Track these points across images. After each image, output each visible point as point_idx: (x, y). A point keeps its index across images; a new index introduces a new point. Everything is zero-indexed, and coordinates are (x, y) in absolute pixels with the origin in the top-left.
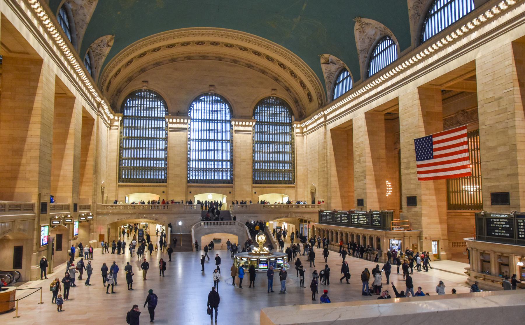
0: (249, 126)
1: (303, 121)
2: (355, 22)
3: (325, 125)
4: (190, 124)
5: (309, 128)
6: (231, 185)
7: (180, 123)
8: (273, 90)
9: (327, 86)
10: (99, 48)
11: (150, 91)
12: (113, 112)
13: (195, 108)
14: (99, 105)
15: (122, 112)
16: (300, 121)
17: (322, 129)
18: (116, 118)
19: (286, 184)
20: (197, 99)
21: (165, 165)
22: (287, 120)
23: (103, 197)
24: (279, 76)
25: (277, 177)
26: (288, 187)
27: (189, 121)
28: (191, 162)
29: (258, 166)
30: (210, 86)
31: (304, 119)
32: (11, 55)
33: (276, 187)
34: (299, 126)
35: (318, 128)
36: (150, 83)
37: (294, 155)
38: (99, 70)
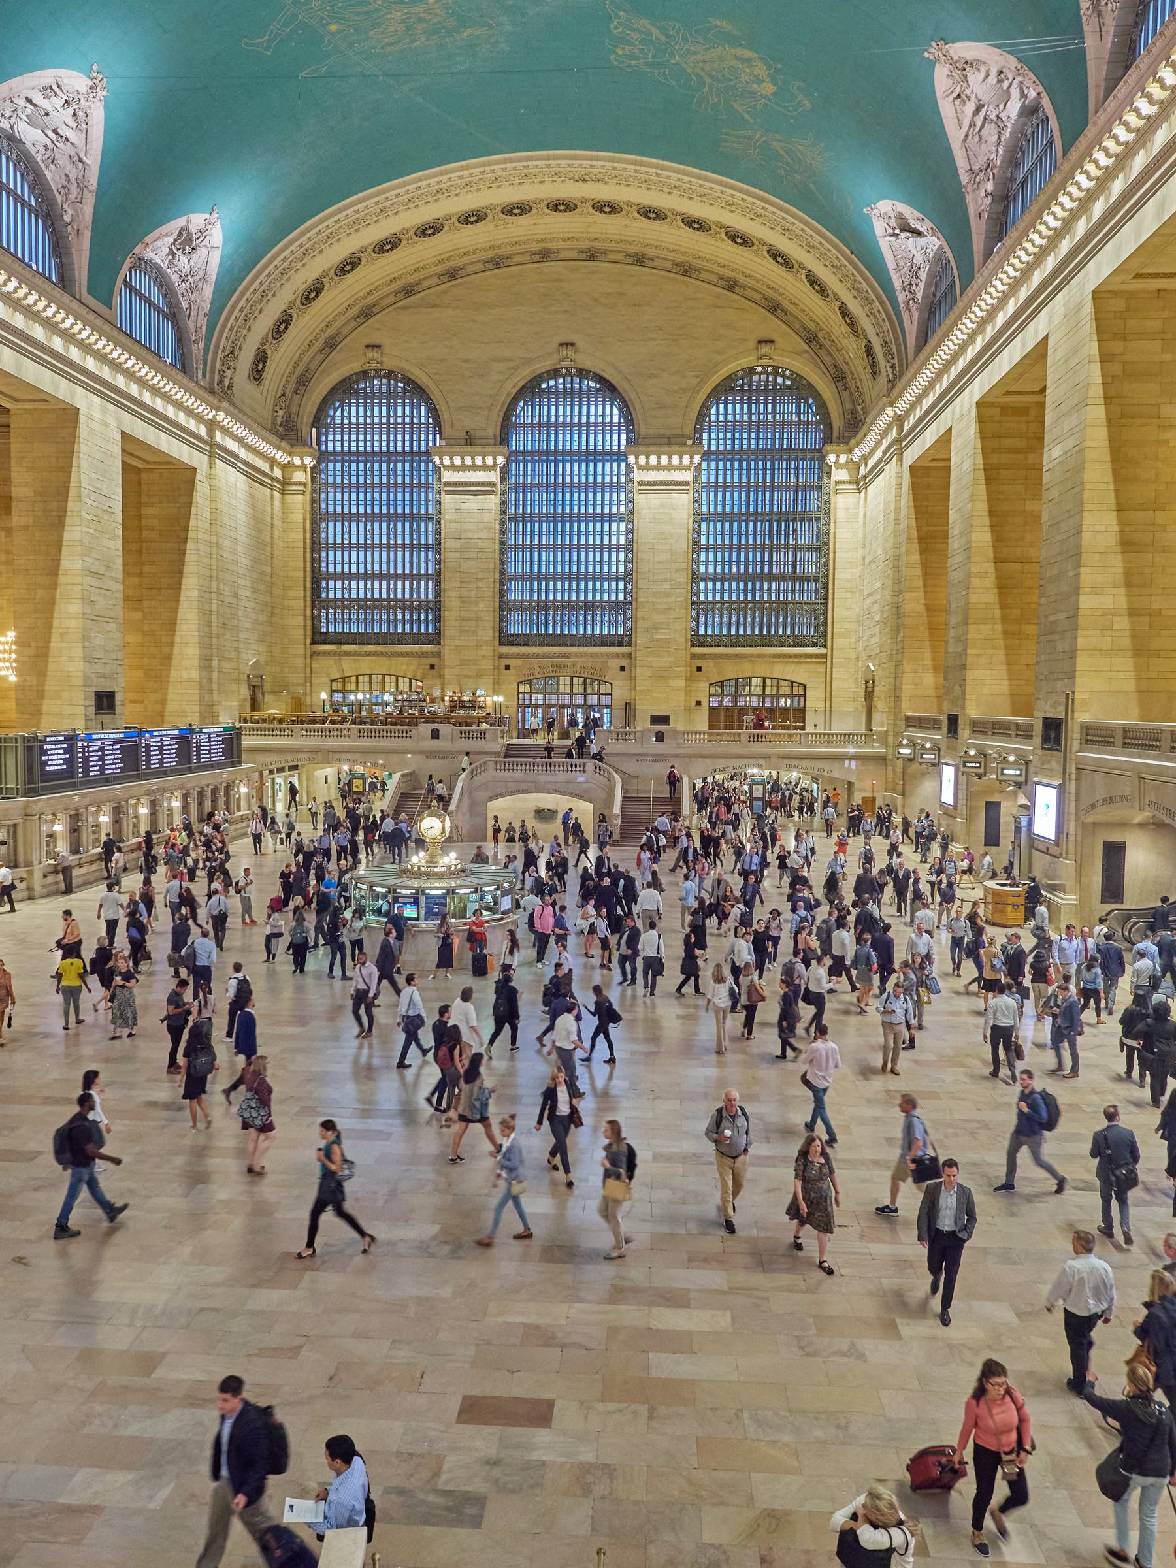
0: (680, 467)
1: (853, 441)
2: (932, 64)
5: (871, 463)
6: (625, 650)
7: (474, 468)
8: (760, 342)
9: (906, 316)
10: (183, 259)
11: (390, 375)
12: (284, 444)
14: (212, 425)
16: (847, 443)
17: (891, 468)
18: (297, 461)
20: (530, 390)
21: (438, 593)
22: (812, 440)
24: (781, 294)
29: (708, 592)
30: (561, 344)
34: (843, 459)
36: (387, 349)
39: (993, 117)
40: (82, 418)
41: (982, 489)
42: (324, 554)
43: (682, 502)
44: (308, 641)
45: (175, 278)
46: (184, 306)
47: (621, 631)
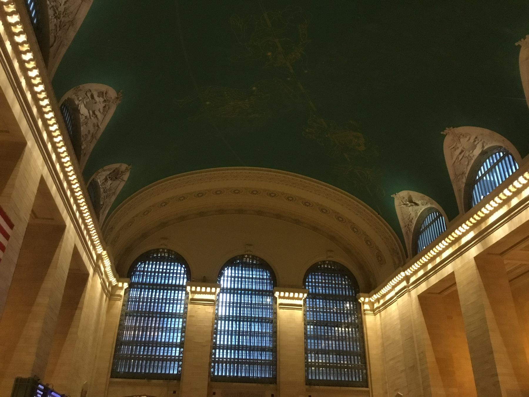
0: (298, 299)
1: (373, 292)
2: (444, 136)
3: (409, 291)
4: (218, 295)
7: (205, 293)
8: (329, 251)
10: (109, 182)
12: (118, 275)
13: (226, 274)
14: (99, 256)
18: (120, 285)
27: (218, 290)
28: (217, 351)
31: (374, 289)
35: (398, 297)
37: (364, 342)
39: (467, 155)
40: (66, 231)
41: (484, 292)
43: (299, 314)
44: (109, 376)
45: (102, 190)
46: (101, 203)
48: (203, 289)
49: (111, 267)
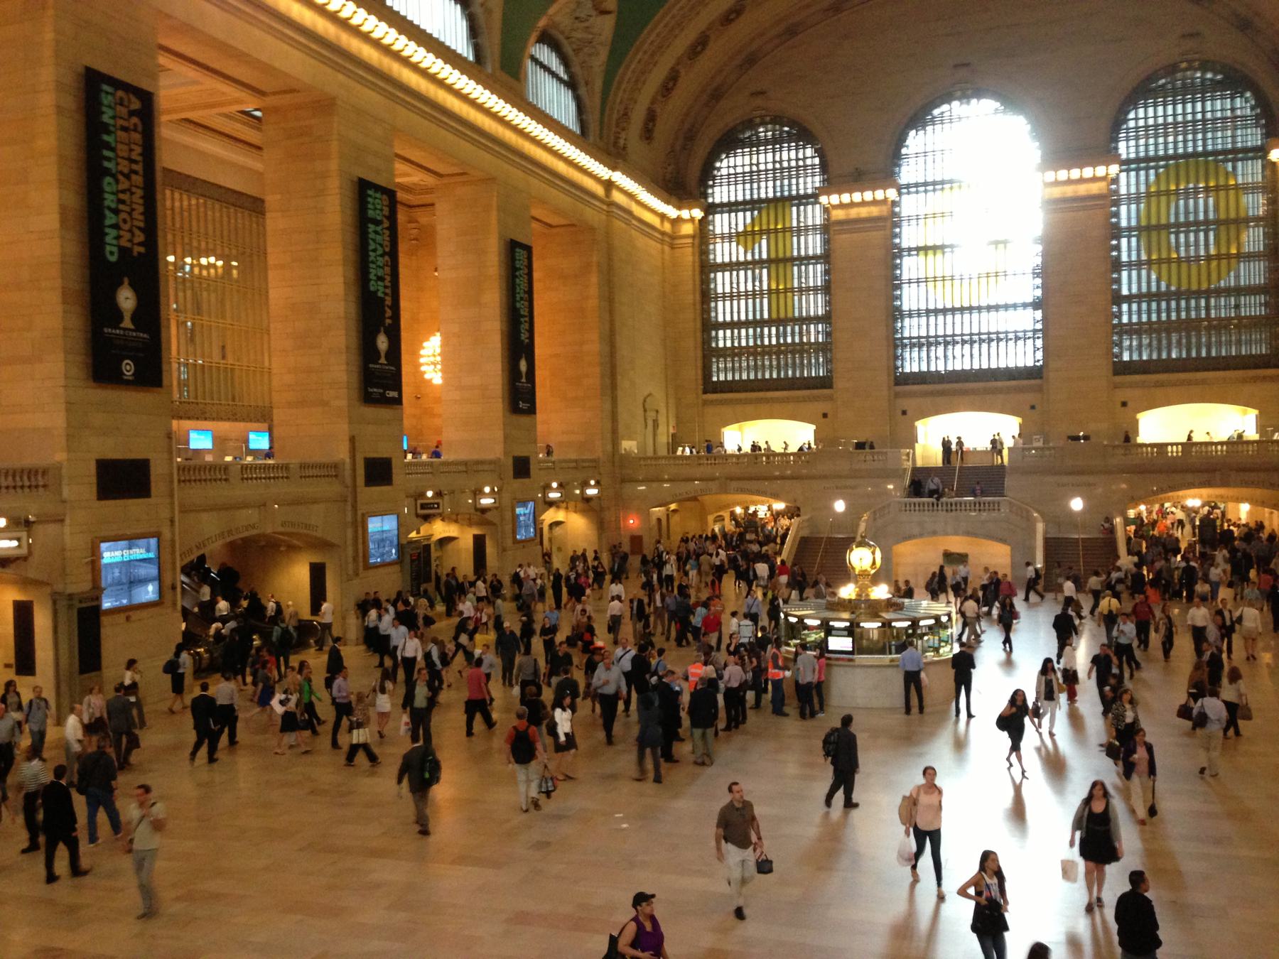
6: (1033, 382)
11: (777, 120)
12: (673, 199)
14: (609, 185)
15: (705, 196)
18: (685, 214)
19: (1245, 367)
21: (828, 334)
23: (655, 435)
25: (1219, 344)
26: (1255, 380)
27: (892, 194)
28: (907, 321)
30: (956, 66)
32: (270, 101)
33: (1204, 382)
38: (598, 84)
42: (713, 304)
47: (1030, 363)
48: (857, 197)
49: (649, 190)
